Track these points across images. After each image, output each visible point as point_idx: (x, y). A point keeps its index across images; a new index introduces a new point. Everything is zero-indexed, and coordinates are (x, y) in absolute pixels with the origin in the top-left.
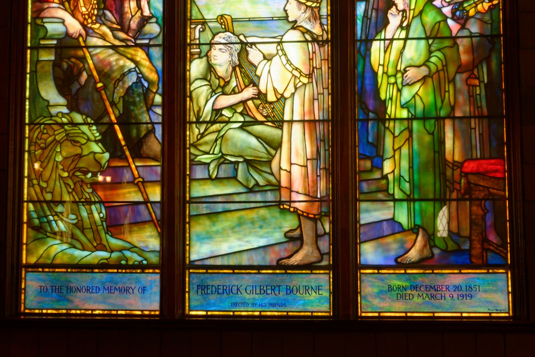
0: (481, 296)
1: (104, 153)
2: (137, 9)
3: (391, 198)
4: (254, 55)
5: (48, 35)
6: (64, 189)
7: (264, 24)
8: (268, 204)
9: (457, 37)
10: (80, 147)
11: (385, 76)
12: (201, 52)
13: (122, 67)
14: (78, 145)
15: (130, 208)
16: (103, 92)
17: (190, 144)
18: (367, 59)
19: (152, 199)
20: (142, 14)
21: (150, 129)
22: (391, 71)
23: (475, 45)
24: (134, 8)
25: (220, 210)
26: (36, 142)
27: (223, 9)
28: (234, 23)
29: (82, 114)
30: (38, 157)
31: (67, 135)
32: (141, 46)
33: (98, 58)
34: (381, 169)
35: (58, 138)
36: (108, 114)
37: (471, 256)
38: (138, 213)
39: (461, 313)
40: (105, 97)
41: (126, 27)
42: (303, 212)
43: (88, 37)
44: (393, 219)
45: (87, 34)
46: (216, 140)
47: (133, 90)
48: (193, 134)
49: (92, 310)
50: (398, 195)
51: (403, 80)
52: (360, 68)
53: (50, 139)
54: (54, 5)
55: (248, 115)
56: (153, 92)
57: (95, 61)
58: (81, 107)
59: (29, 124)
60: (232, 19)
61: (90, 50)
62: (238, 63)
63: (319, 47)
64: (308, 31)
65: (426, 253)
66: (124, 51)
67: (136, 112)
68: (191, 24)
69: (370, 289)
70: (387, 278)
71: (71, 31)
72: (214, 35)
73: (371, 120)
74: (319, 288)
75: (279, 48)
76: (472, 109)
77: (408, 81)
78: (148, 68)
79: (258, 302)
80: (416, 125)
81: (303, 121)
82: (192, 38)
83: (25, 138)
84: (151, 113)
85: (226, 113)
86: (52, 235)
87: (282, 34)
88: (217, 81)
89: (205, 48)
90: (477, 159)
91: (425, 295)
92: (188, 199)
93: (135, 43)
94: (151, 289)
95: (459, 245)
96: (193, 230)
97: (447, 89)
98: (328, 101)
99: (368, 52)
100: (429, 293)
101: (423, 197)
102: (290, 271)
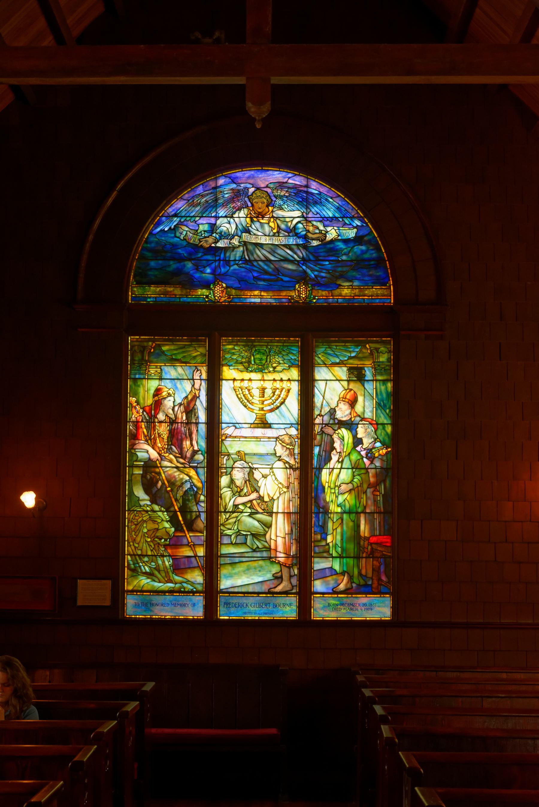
0: (377, 609)
1: (171, 528)
4: (257, 475)
6: (148, 548)
7: (262, 457)
9: (368, 468)
10: (157, 524)
12: (227, 472)
13: (182, 479)
14: (156, 523)
15: (186, 560)
16: (171, 493)
18: (320, 479)
19: (199, 554)
20: (193, 448)
22: (332, 486)
23: (378, 473)
25: (237, 561)
26: (132, 521)
27: (239, 447)
29: (158, 505)
30: (133, 529)
31: (150, 517)
32: (193, 467)
33: (168, 473)
35: (144, 519)
36: (173, 506)
37: (372, 588)
38: (191, 562)
39: (366, 618)
40: (171, 496)
41: (184, 456)
42: (283, 563)
44: (331, 568)
45: (162, 459)
46: (235, 522)
47: (188, 493)
49: (165, 616)
50: (335, 554)
52: (316, 484)
53: (140, 519)
55: (253, 508)
58: (158, 502)
59: (128, 511)
61: (163, 468)
62: (248, 479)
64: (287, 462)
65: (349, 586)
67: (190, 505)
68: (221, 456)
69: (318, 605)
70: (327, 600)
71: (152, 457)
72: (234, 462)
73: (321, 513)
74: (291, 605)
75: (271, 471)
76: (375, 508)
77: (341, 492)
78: (197, 480)
79: (258, 612)
80: (345, 516)
81: (284, 513)
83: (125, 518)
86: (141, 574)
88: (236, 489)
89: (230, 470)
90: (377, 536)
91: (347, 609)
93: (189, 465)
94: (198, 604)
95: (366, 582)
96: (222, 572)
97: (362, 497)
98: (297, 501)
100: (349, 607)
101: (348, 556)
102: (275, 595)
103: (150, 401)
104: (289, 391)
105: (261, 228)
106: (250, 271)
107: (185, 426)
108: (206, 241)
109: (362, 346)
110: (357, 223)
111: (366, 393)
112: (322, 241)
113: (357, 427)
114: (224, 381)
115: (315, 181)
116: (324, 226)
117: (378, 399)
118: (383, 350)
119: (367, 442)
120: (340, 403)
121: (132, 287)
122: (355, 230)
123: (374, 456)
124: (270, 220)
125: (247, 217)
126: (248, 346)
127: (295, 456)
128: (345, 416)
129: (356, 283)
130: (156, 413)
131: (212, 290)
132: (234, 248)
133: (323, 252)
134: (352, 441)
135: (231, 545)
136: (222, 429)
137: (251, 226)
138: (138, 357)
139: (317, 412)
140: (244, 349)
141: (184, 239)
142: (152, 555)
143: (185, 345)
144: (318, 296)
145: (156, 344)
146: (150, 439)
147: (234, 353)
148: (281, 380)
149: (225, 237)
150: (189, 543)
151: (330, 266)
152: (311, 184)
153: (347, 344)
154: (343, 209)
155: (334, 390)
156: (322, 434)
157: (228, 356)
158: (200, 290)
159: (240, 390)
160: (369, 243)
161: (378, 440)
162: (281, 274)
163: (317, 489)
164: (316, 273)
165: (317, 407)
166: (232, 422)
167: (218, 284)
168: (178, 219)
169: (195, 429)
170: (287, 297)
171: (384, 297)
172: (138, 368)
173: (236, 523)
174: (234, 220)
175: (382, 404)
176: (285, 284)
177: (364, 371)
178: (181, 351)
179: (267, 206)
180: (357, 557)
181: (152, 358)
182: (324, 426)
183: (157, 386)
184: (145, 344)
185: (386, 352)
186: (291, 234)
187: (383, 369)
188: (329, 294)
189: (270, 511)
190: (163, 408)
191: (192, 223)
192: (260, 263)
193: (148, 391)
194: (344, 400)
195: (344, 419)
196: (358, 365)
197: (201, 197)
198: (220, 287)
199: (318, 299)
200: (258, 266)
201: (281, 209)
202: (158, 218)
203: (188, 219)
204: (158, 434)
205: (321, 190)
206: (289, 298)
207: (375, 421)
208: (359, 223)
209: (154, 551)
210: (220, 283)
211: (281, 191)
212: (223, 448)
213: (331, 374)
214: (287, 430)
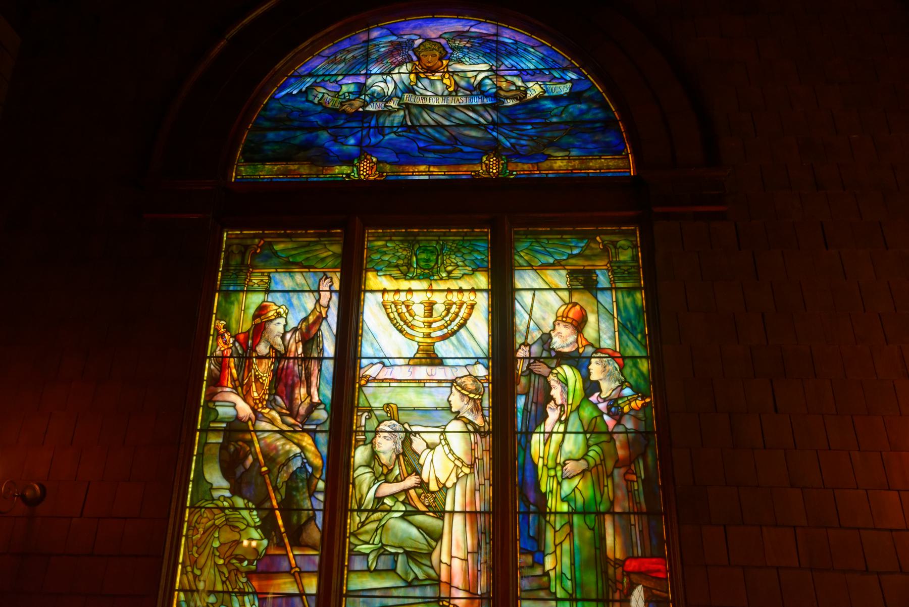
1: (262, 539)
2: (307, 395)
3: (553, 597)
4: (418, 444)
5: (218, 418)
7: (428, 414)
8: (427, 600)
10: (239, 532)
11: (545, 469)
12: (366, 439)
13: (288, 452)
14: (237, 530)
15: (284, 600)
16: (267, 476)
17: (350, 533)
18: (528, 451)
20: (311, 400)
21: (311, 515)
22: (551, 464)
23: (631, 440)
24: (304, 395)
26: (195, 527)
27: (389, 398)
28: (400, 412)
29: (244, 498)
30: (195, 542)
31: (227, 520)
32: (308, 432)
33: (265, 442)
34: (543, 564)
35: (217, 522)
36: (270, 499)
40: (268, 481)
41: (295, 413)
43: (257, 421)
45: (257, 419)
46: (377, 529)
47: (297, 475)
48: (354, 522)
50: (560, 594)
51: (562, 473)
52: (521, 460)
53: (210, 523)
54: (228, 389)
55: (410, 504)
56: (316, 478)
57: (262, 445)
60: (398, 408)
61: (258, 434)
62: (401, 451)
63: (481, 438)
64: (470, 422)
66: (291, 436)
67: (298, 498)
68: (358, 412)
71: (241, 415)
72: (380, 423)
73: (532, 513)
76: (631, 505)
77: (568, 475)
78: (313, 453)
80: (576, 519)
81: (464, 512)
82: (359, 425)
84: (313, 499)
85: (388, 501)
87: (445, 424)
88: (381, 468)
92: (344, 592)
93: (302, 428)
97: (606, 484)
98: (488, 491)
99: (528, 444)
101: (585, 597)
103: (247, 325)
104: (472, 307)
105: (432, 86)
106: (414, 140)
107: (300, 363)
108: (351, 105)
109: (589, 239)
110: (572, 76)
111: (601, 310)
112: (520, 99)
113: (590, 363)
114: (368, 295)
115: (508, 28)
116: (523, 81)
117: (621, 318)
118: (624, 245)
119: (607, 388)
120: (559, 324)
121: (237, 166)
122: (569, 85)
123: (622, 412)
124: (444, 76)
125: (410, 73)
126: (408, 241)
127: (484, 411)
128: (568, 345)
129: (574, 153)
130: (256, 344)
131: (356, 166)
132: (391, 112)
133: (523, 113)
134: (582, 385)
135: (367, 574)
136: (361, 368)
137: (416, 85)
138: (236, 260)
139: (519, 340)
140: (401, 246)
141: (320, 104)
142: (223, 592)
143: (310, 242)
144: (516, 171)
145: (265, 242)
146: (242, 385)
147: (385, 252)
148: (461, 290)
149: (378, 99)
150: (292, 568)
151: (533, 131)
152: (503, 32)
153: (564, 237)
154: (551, 60)
155: (547, 304)
156: (530, 375)
157: (375, 257)
158: (338, 167)
159: (393, 306)
160: (591, 100)
161: (626, 384)
162: (459, 143)
163: (523, 469)
164: (513, 141)
165: (520, 331)
166: (377, 356)
167: (365, 158)
168: (313, 80)
169: (316, 368)
170: (469, 173)
171: (619, 170)
172: (234, 276)
173: (379, 532)
174: (392, 78)
175: (629, 326)
176: (466, 156)
177: (595, 275)
178: (303, 250)
179: (441, 59)
181: (257, 262)
182: (532, 361)
183: (260, 302)
184: (249, 242)
185: (629, 247)
186: (474, 93)
187: (626, 272)
188: (533, 167)
189: (439, 509)
190: (267, 335)
191: (331, 84)
192: (429, 130)
193: (246, 311)
194: (564, 319)
195: (566, 350)
196: (584, 266)
197: (346, 52)
198: (368, 162)
199: (517, 174)
200: (426, 135)
201: (459, 63)
202: (286, 78)
203: (327, 78)
204: (255, 376)
205: (518, 38)
206: (473, 174)
207: (619, 352)
208: (574, 76)
209: (228, 583)
210: (368, 157)
211: (460, 42)
212: (361, 400)
213: (540, 280)
214: (469, 368)
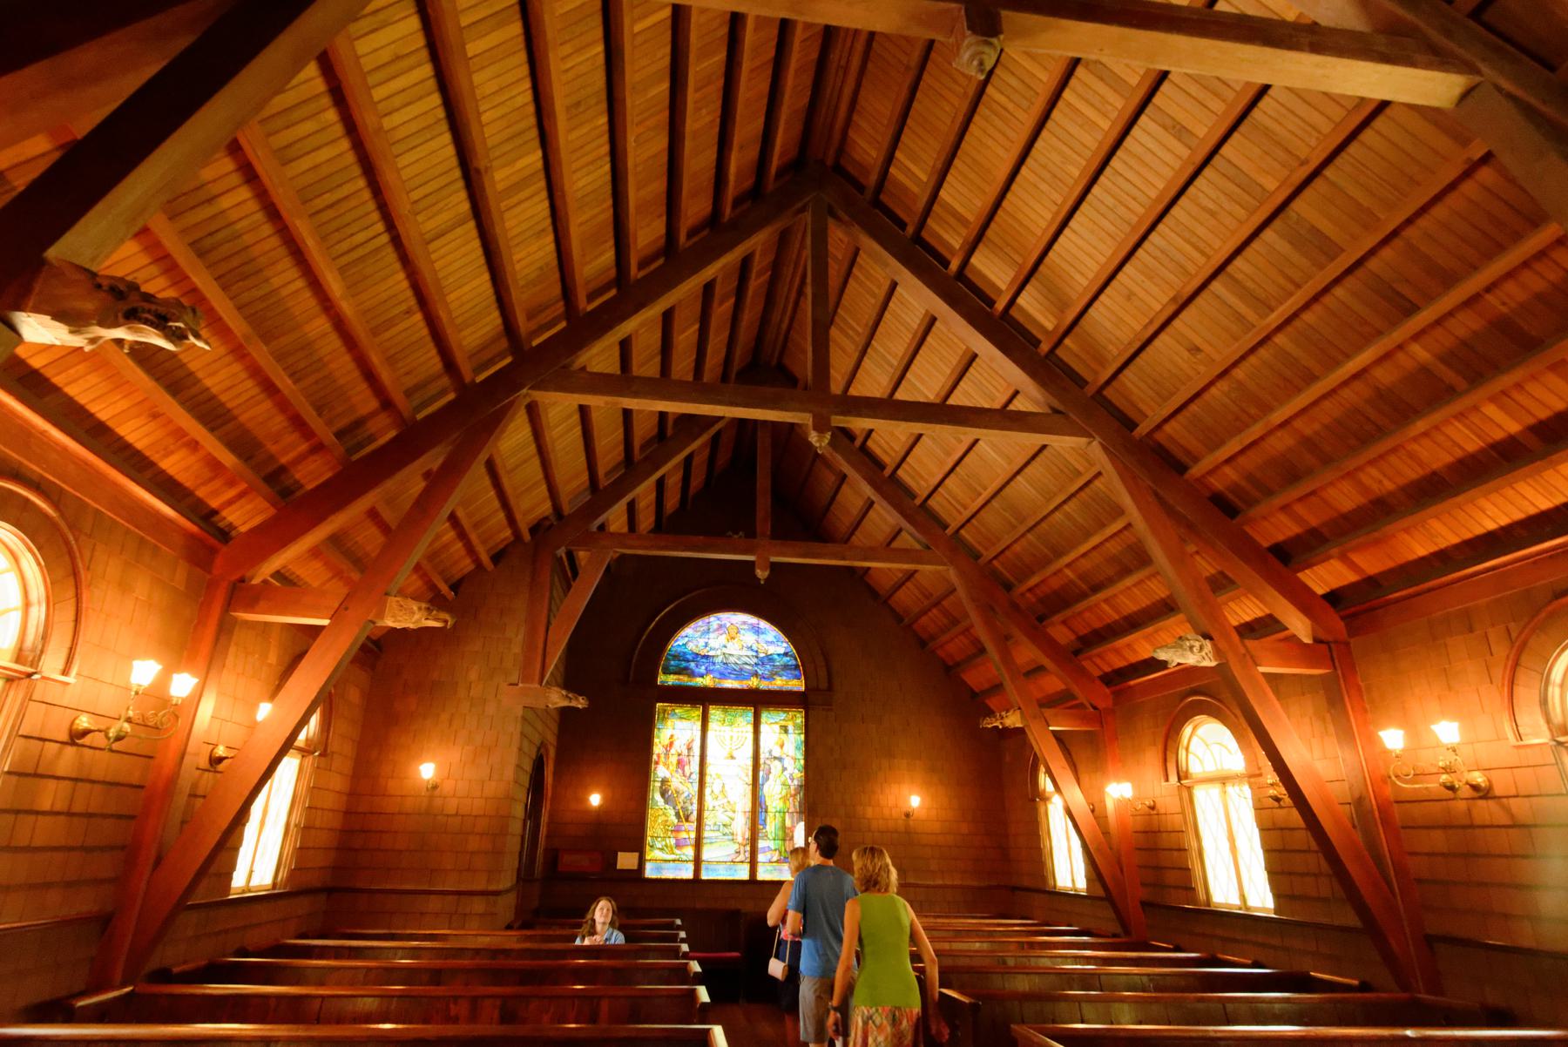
4: (727, 788)
85: (717, 808)
103: (667, 742)
110: (785, 645)
138: (661, 715)
160: (791, 656)
180: (784, 840)
